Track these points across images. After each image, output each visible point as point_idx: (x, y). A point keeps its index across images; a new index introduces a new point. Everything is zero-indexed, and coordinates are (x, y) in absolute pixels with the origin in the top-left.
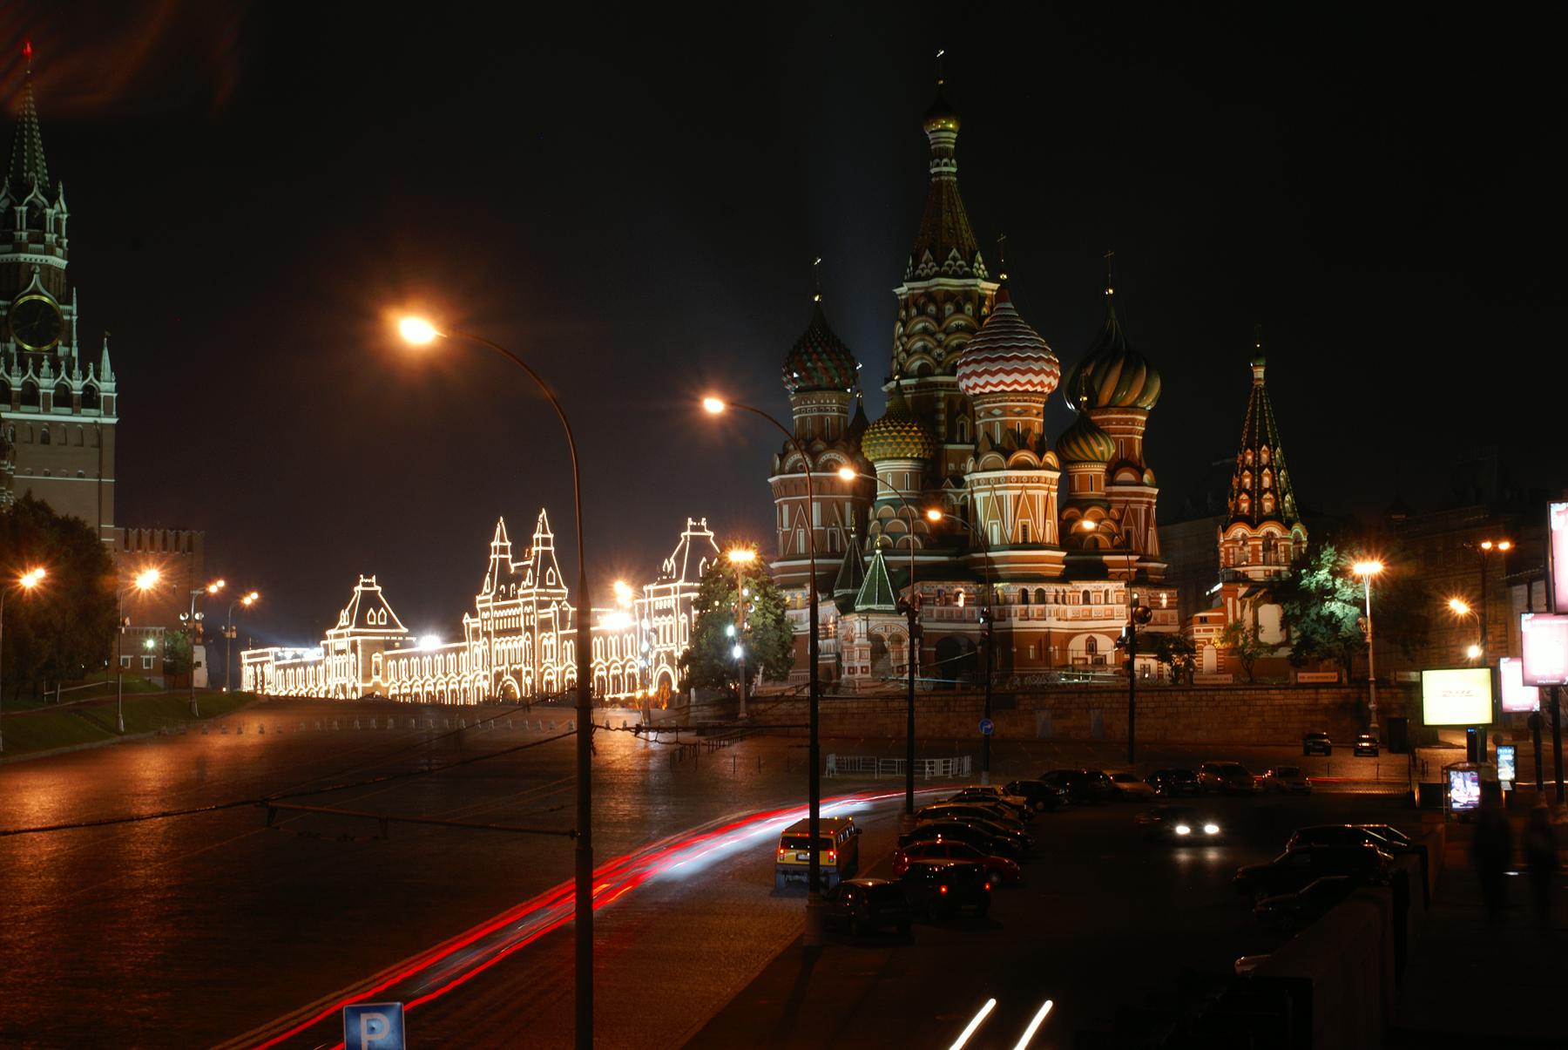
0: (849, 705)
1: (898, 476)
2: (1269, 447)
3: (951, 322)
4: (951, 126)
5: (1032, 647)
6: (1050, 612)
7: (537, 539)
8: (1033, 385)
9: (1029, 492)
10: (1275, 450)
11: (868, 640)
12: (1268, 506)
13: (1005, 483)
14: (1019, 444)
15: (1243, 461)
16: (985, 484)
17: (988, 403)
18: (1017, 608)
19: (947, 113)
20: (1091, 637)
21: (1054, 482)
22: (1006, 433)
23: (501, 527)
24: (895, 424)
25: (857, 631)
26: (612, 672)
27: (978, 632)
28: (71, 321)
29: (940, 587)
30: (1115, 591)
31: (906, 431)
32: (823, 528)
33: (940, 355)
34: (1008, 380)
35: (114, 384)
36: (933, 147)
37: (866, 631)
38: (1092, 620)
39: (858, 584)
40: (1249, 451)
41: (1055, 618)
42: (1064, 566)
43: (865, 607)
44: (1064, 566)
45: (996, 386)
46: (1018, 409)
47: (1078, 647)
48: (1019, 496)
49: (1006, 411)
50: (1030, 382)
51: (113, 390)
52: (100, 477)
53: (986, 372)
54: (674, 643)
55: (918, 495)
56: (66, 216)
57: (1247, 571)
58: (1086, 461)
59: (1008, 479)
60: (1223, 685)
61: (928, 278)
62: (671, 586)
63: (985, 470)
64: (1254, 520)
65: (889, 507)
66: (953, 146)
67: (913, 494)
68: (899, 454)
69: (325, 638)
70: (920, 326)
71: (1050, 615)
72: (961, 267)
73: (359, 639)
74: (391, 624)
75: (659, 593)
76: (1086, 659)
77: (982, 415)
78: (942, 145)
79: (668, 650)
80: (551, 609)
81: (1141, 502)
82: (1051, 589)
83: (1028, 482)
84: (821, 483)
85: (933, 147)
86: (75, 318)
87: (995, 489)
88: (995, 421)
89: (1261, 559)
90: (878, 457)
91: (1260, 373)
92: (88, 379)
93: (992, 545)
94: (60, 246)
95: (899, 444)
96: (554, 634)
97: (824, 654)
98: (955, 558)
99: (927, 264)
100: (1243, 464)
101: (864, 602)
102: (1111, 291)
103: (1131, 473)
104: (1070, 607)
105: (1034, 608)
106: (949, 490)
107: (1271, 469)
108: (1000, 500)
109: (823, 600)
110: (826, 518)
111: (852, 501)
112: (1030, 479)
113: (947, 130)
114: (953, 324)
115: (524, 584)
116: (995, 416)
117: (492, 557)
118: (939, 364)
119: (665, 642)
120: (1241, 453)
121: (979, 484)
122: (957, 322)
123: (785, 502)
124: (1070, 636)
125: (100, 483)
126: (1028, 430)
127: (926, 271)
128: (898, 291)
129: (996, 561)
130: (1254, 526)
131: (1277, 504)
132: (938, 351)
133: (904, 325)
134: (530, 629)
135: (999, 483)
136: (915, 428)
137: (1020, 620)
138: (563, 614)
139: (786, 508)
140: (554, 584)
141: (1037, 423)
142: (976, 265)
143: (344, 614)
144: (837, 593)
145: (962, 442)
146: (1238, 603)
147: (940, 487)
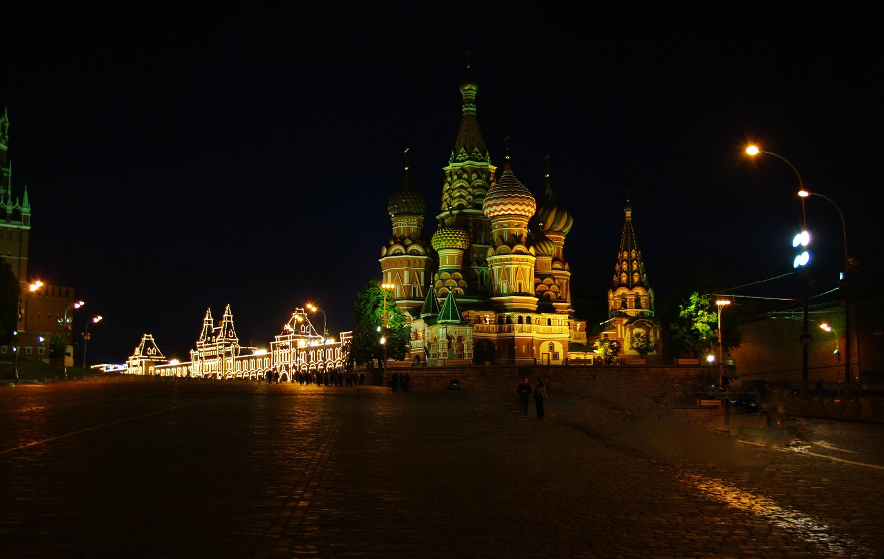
0: (442, 372)
1: (451, 258)
2: (635, 250)
3: (475, 183)
4: (474, 88)
5: (524, 347)
6: (533, 328)
7: (225, 317)
8: (525, 212)
9: (523, 266)
10: (638, 252)
11: (447, 339)
12: (636, 279)
14: (517, 241)
15: (622, 257)
16: (499, 262)
17: (501, 220)
19: (472, 82)
20: (551, 342)
21: (533, 262)
22: (510, 237)
23: (209, 311)
24: (451, 230)
25: (441, 333)
26: (258, 374)
27: (495, 338)
28: (8, 177)
29: (477, 313)
30: (563, 319)
31: (457, 234)
32: (410, 284)
33: (470, 199)
34: (513, 208)
35: (29, 209)
36: (464, 98)
39: (435, 311)
40: (625, 252)
41: (536, 332)
42: (537, 306)
43: (444, 321)
44: (537, 306)
45: (506, 211)
46: (516, 224)
47: (544, 348)
48: (518, 268)
49: (510, 225)
50: (523, 210)
51: (29, 212)
52: (19, 256)
53: (501, 203)
54: (289, 361)
55: (461, 268)
56: (8, 124)
58: (543, 255)
60: (640, 365)
61: (463, 161)
62: (288, 336)
64: (630, 286)
65: (448, 273)
66: (474, 98)
67: (458, 267)
68: (453, 246)
69: (128, 360)
70: (458, 185)
71: (533, 330)
72: (479, 156)
73: (144, 360)
74: (158, 354)
75: (282, 339)
76: (549, 354)
77: (496, 227)
78: (470, 97)
79: (286, 364)
80: (231, 347)
81: (564, 279)
82: (534, 316)
83: (522, 261)
84: (409, 261)
85: (464, 98)
86: (10, 175)
87: (505, 264)
89: (634, 306)
90: (441, 247)
91: (628, 214)
92: (16, 206)
93: (503, 293)
94: (4, 139)
95: (453, 240)
96: (232, 358)
97: (414, 348)
98: (481, 301)
99: (462, 154)
100: (622, 259)
101: (443, 318)
102: (548, 176)
103: (560, 264)
104: (541, 326)
105: (526, 326)
106: (475, 267)
107: (637, 261)
108: (508, 270)
109: (414, 320)
110: (412, 280)
111: (425, 271)
112: (523, 260)
113: (470, 90)
114: (476, 185)
115: (219, 336)
116: (504, 227)
117: (205, 325)
118: (469, 203)
119: (284, 360)
120: (621, 253)
121: (496, 262)
122: (478, 183)
123: (389, 271)
124: (541, 342)
125: (20, 260)
126: (521, 235)
127: (461, 158)
128: (445, 169)
130: (631, 289)
131: (640, 278)
132: (469, 197)
133: (450, 184)
134: (221, 356)
135: (508, 261)
136: (461, 233)
137: (519, 332)
138: (236, 350)
139: (389, 274)
140: (232, 336)
141: (525, 232)
142: (486, 156)
143: (137, 350)
144: (422, 316)
145: (480, 244)
146: (623, 328)
147: (471, 265)
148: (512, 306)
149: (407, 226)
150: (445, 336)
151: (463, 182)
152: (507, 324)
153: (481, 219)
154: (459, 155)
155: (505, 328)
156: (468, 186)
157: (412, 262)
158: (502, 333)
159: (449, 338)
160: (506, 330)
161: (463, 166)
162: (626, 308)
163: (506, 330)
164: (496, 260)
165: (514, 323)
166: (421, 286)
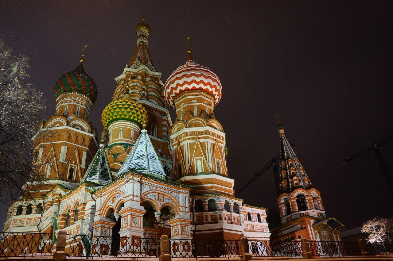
11: (141, 205)
13: (206, 134)
16: (191, 135)
17: (189, 96)
18: (225, 213)
32: (66, 162)
33: (144, 94)
37: (139, 195)
38: (254, 231)
48: (214, 145)
57: (308, 213)
59: (207, 132)
63: (190, 126)
68: (130, 116)
78: (144, 34)
84: (70, 134)
87: (199, 138)
88: (193, 106)
108: (203, 145)
110: (70, 157)
111: (88, 152)
121: (187, 135)
129: (203, 183)
132: (144, 92)
135: (202, 134)
137: (228, 223)
148: (212, 187)
149: (74, 103)
150: (138, 199)
151: (137, 82)
152: (210, 210)
153: (155, 114)
154: (134, 65)
155: (207, 217)
156: (142, 84)
157: (73, 137)
158: (203, 223)
159: (147, 205)
160: (209, 219)
162: (305, 208)
163: (209, 219)
164: (186, 134)
165: (221, 210)
166: (81, 168)
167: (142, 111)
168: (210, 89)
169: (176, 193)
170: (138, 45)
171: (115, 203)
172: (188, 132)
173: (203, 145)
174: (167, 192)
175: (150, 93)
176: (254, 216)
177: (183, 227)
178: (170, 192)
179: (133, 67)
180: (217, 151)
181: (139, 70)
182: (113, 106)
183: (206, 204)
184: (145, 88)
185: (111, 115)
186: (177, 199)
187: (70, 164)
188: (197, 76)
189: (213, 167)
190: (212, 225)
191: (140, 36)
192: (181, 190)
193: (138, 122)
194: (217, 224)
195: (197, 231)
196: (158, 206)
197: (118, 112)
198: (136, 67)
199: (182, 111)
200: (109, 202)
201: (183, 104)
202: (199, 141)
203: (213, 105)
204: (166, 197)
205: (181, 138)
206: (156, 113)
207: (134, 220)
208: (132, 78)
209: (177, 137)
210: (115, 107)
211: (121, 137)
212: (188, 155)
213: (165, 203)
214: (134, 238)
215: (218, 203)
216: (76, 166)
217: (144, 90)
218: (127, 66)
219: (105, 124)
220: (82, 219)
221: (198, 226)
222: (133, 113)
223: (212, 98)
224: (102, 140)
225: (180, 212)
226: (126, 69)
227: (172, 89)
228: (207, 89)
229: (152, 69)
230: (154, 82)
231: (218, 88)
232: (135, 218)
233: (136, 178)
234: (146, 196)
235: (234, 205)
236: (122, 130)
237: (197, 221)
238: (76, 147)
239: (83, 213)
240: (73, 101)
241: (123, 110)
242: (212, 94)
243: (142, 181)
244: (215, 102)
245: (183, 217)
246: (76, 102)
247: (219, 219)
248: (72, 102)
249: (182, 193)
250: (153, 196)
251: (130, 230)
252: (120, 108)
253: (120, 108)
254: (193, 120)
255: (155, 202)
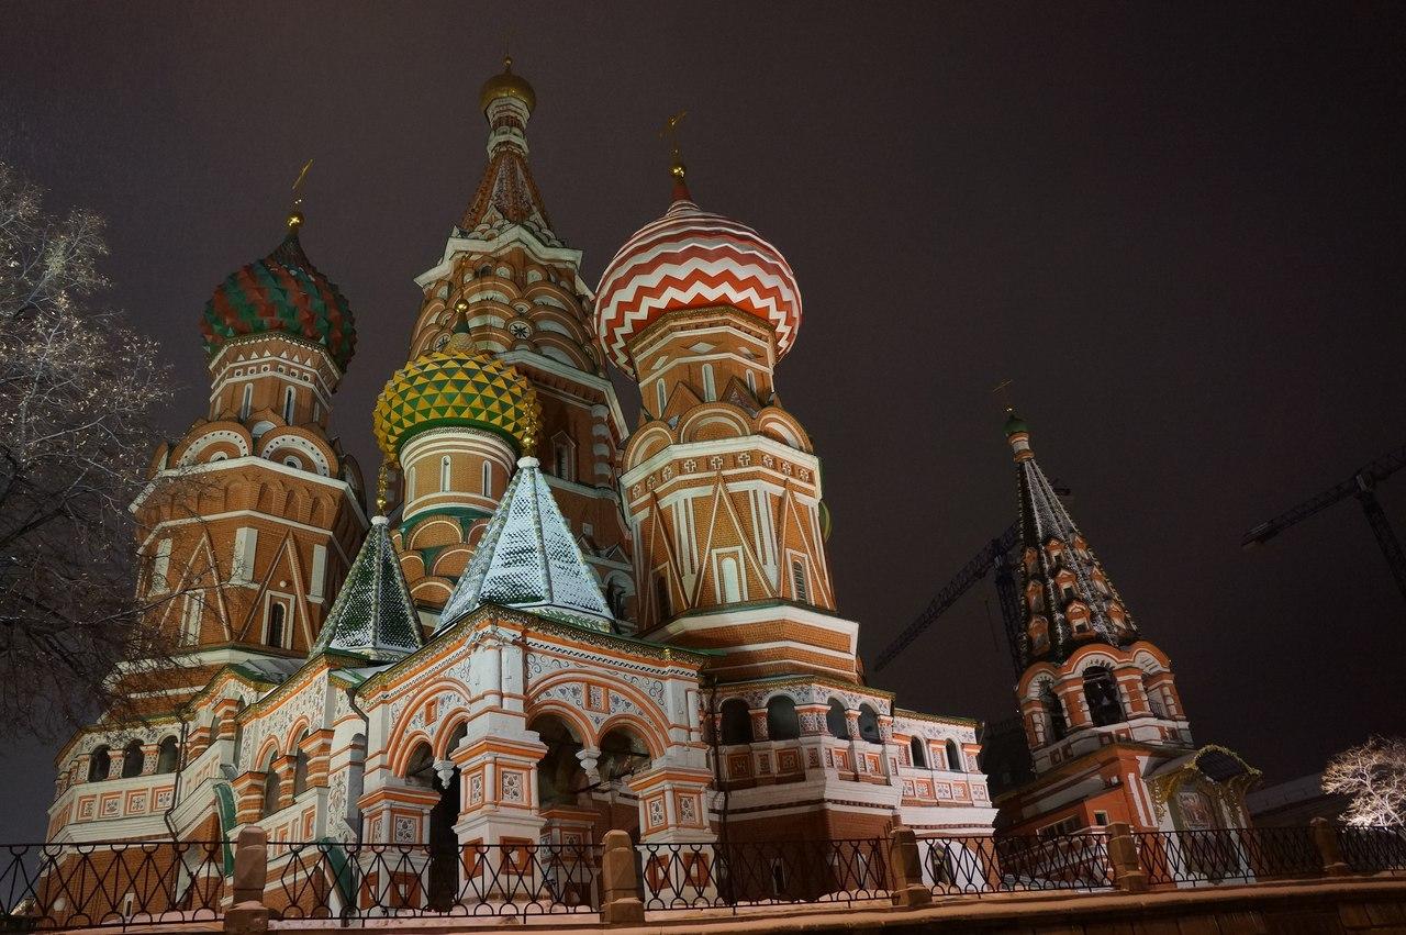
16: (696, 471)
18: (830, 743)
25: (489, 684)
33: (521, 331)
38: (938, 805)
48: (781, 500)
57: (1126, 731)
59: (755, 457)
63: (692, 438)
68: (476, 412)
78: (512, 114)
84: (264, 487)
87: (726, 479)
108: (739, 501)
110: (268, 565)
111: (330, 546)
132: (520, 324)
135: (736, 465)
137: (842, 778)
148: (781, 654)
150: (519, 706)
151: (495, 288)
152: (774, 735)
153: (564, 399)
154: (481, 227)
155: (765, 760)
157: (277, 494)
158: (754, 784)
159: (553, 729)
160: (775, 769)
161: (496, 251)
162: (1113, 713)
163: (775, 769)
164: (679, 466)
165: (816, 733)
167: (517, 391)
168: (758, 303)
169: (653, 680)
170: (492, 155)
171: (437, 725)
172: (685, 460)
173: (739, 501)
174: (620, 675)
175: (545, 325)
176: (934, 749)
177: (681, 800)
178: (629, 676)
179: (479, 234)
180: (792, 522)
181: (501, 245)
182: (414, 378)
183: (762, 714)
184: (525, 307)
185: (407, 409)
186: (655, 700)
187: (269, 593)
188: (709, 257)
189: (779, 581)
190: (787, 786)
191: (499, 123)
192: (670, 667)
193: (506, 432)
194: (802, 784)
195: (734, 812)
196: (590, 727)
197: (431, 398)
198: (489, 232)
199: (661, 387)
200: (414, 721)
201: (663, 359)
202: (726, 490)
203: (771, 360)
204: (617, 694)
205: (662, 481)
206: (568, 397)
207: (506, 781)
208: (476, 275)
209: (646, 479)
210: (420, 381)
211: (447, 487)
212: (690, 541)
213: (612, 715)
214: (507, 845)
215: (803, 707)
216: (292, 598)
217: (521, 315)
218: (456, 231)
219: (388, 442)
220: (322, 785)
221: (734, 793)
222: (487, 401)
223: (764, 332)
224: (380, 501)
225: (669, 744)
226: (455, 244)
227: (623, 307)
228: (748, 301)
229: (546, 240)
230: (557, 284)
231: (787, 295)
232: (510, 776)
233: (506, 633)
234: (544, 695)
235: (860, 713)
236: (449, 460)
237: (733, 775)
238: (288, 530)
239: (324, 766)
240: (268, 366)
241: (449, 389)
242: (767, 320)
243: (529, 640)
244: (777, 349)
245: (681, 763)
246: (281, 370)
247: (811, 767)
248: (265, 369)
249: (673, 677)
250: (569, 694)
251: (492, 818)
252: (440, 385)
253: (440, 385)
254: (703, 417)
255: (577, 713)
